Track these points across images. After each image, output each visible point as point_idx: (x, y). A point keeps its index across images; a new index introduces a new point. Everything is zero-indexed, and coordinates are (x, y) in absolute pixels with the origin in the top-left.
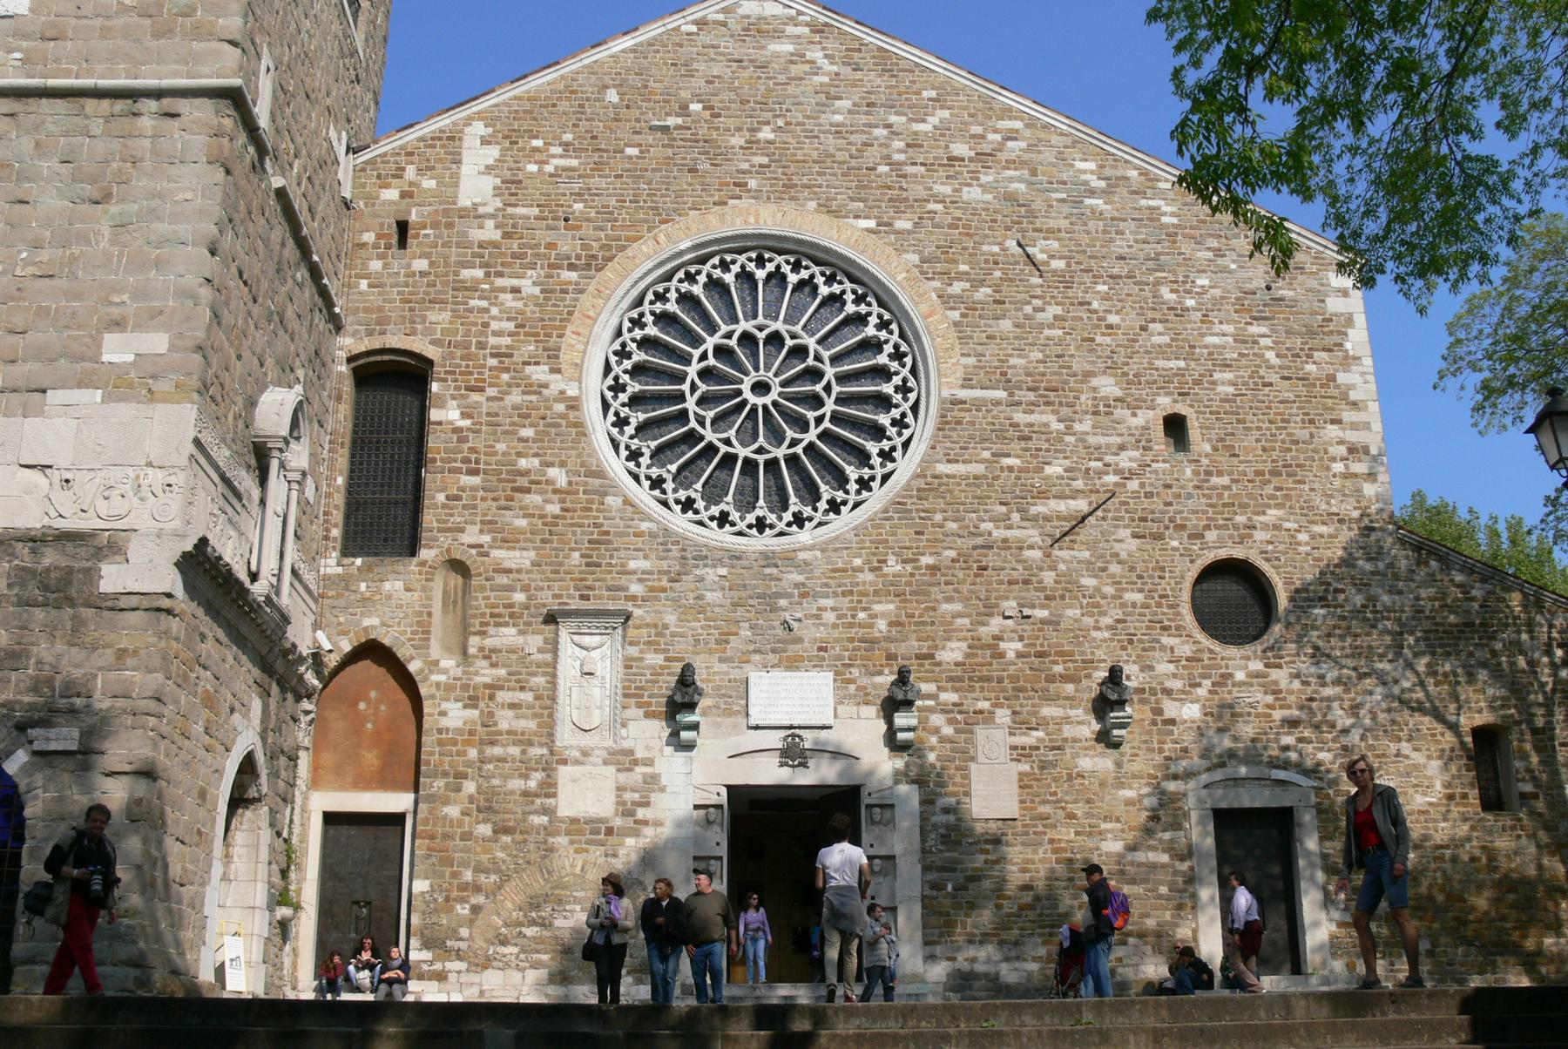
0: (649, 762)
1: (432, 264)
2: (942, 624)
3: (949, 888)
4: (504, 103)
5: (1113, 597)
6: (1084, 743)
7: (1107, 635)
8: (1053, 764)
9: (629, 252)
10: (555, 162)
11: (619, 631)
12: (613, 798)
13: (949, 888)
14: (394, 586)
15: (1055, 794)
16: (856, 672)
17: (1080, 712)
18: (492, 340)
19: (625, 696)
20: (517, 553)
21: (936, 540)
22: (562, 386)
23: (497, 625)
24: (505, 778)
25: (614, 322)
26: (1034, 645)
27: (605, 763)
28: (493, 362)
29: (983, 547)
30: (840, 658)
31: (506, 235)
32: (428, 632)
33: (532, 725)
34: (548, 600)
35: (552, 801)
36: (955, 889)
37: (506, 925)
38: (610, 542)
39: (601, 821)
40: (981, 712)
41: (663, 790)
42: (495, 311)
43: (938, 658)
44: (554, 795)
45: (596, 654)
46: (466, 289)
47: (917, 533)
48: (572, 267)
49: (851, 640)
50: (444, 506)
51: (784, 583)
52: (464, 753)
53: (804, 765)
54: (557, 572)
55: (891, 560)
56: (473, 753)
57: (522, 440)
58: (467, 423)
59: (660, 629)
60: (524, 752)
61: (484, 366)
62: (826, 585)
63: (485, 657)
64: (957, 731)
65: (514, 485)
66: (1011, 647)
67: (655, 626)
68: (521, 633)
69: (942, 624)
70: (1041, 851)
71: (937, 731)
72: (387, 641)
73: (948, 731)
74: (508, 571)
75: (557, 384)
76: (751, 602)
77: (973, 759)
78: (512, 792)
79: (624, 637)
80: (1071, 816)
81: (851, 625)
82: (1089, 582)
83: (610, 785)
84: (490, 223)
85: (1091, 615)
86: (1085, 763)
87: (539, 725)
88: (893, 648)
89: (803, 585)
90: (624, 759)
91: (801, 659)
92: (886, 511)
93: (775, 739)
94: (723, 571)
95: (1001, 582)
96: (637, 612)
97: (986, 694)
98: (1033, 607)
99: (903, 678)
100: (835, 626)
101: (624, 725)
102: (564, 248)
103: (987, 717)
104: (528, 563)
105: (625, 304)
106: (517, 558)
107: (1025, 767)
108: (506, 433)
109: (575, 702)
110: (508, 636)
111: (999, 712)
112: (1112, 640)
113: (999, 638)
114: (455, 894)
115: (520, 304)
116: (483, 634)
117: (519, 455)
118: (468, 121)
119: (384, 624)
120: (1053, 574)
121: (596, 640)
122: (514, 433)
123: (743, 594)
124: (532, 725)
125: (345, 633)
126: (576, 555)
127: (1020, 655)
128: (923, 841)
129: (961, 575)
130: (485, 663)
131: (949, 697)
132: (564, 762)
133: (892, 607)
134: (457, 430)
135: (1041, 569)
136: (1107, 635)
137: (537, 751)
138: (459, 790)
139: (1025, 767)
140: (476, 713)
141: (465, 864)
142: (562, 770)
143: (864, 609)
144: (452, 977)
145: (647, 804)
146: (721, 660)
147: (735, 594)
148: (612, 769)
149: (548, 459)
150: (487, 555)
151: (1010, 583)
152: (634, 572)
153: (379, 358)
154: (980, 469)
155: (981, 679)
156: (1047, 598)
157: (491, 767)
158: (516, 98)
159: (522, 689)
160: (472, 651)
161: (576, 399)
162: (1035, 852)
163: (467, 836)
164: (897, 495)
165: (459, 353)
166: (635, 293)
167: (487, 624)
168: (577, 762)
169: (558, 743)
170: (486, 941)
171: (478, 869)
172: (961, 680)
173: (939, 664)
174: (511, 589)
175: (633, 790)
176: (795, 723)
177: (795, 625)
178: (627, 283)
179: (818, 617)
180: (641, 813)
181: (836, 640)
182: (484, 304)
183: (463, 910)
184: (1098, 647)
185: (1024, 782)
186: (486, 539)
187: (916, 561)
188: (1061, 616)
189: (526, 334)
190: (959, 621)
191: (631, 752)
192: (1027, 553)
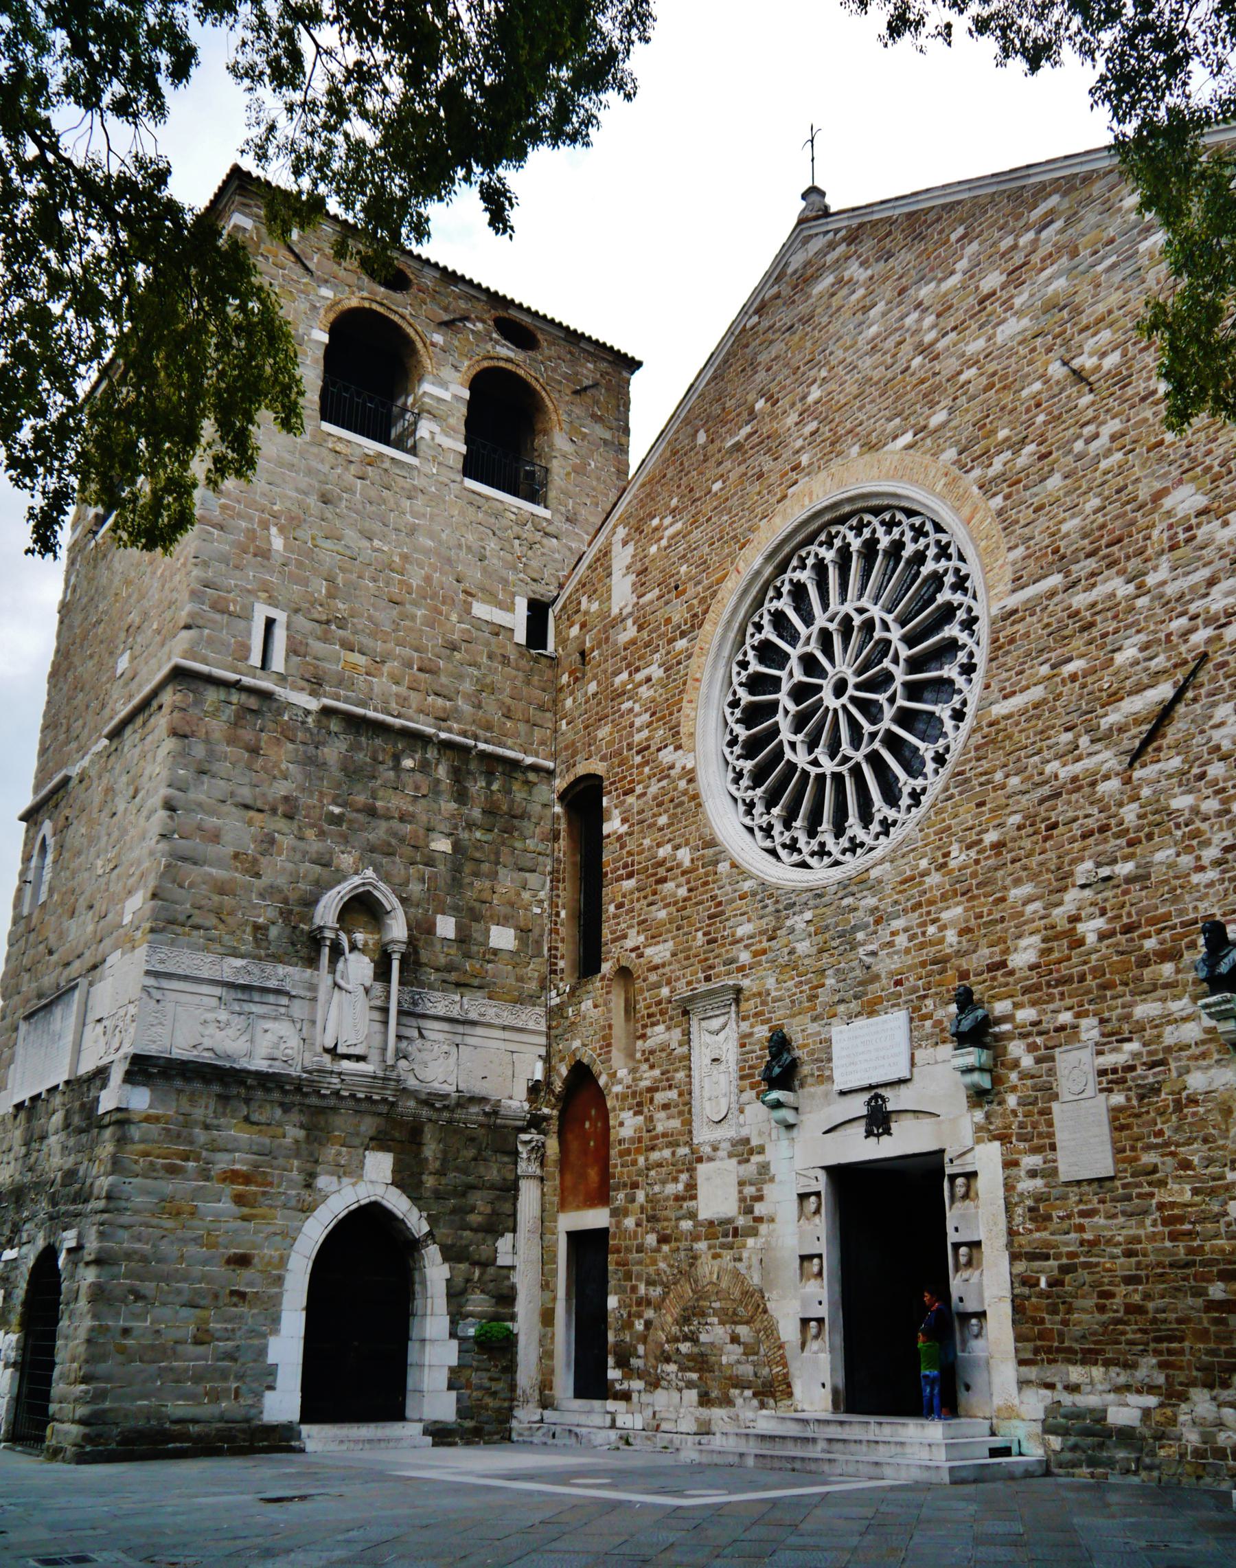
0: (761, 1150)
1: (599, 684)
2: (1013, 917)
3: (1043, 1284)
4: (635, 496)
5: (1219, 814)
6: (1195, 1051)
7: (1212, 874)
8: (1157, 1091)
9: (719, 596)
10: (668, 533)
11: (733, 1008)
12: (735, 1196)
13: (1043, 1284)
14: (587, 1005)
15: (1160, 1133)
16: (929, 1002)
17: (1186, 1000)
18: (638, 738)
19: (742, 1078)
20: (660, 947)
21: (1000, 807)
22: (683, 761)
23: (653, 1024)
24: (664, 1182)
25: (721, 672)
26: (1119, 917)
27: (730, 1155)
28: (638, 759)
29: (1049, 798)
30: (915, 990)
31: (640, 629)
32: (609, 1045)
33: (676, 1123)
34: (683, 991)
35: (693, 1203)
36: (1050, 1285)
37: (668, 1341)
38: (722, 913)
39: (729, 1221)
40: (1062, 1028)
41: (772, 1180)
42: (637, 708)
43: (1011, 965)
44: (694, 1197)
45: (722, 1035)
46: (619, 696)
47: (981, 804)
48: (683, 634)
49: (923, 964)
50: (616, 916)
51: (860, 914)
52: (634, 1163)
53: (888, 1132)
54: (687, 958)
55: (955, 850)
56: (641, 1160)
57: (661, 829)
58: (626, 826)
59: (762, 995)
60: (673, 1154)
61: (632, 767)
62: (896, 902)
63: (647, 1060)
64: (1038, 1061)
65: (658, 873)
66: (1090, 929)
67: (760, 994)
68: (668, 1028)
69: (1013, 917)
70: (1148, 1222)
71: (1016, 1064)
72: (585, 1060)
73: (1027, 1061)
74: (656, 968)
75: (683, 760)
76: (834, 944)
77: (1055, 1097)
78: (667, 1199)
79: (738, 1013)
80: (1186, 1165)
81: (922, 946)
82: (1182, 802)
83: (734, 1181)
84: (630, 622)
85: (1189, 849)
86: (1196, 1081)
87: (683, 1124)
88: (964, 964)
89: (877, 908)
90: (744, 1150)
91: (878, 1000)
92: (946, 789)
93: (858, 1106)
94: (808, 915)
95: (1073, 840)
96: (745, 983)
97: (1068, 1002)
98: (1114, 861)
99: (965, 1000)
100: (907, 951)
101: (742, 1111)
102: (676, 619)
103: (1068, 1033)
104: (668, 954)
105: (726, 653)
106: (659, 952)
107: (1118, 1099)
108: (650, 826)
109: (706, 1094)
110: (659, 1034)
111: (1085, 1023)
112: (1222, 880)
113: (1075, 919)
114: (634, 1309)
115: (651, 692)
116: (643, 1037)
117: (659, 845)
118: (613, 532)
119: (584, 1045)
120: (1135, 805)
121: (722, 1020)
122: (654, 824)
123: (827, 935)
124: (676, 1123)
125: (562, 1060)
126: (700, 934)
127: (1102, 936)
128: (1010, 1218)
129: (1027, 843)
130: (645, 1067)
131: (1026, 1015)
132: (700, 1160)
133: (959, 910)
134: (620, 838)
135: (1120, 805)
136: (1212, 874)
137: (683, 1151)
138: (633, 1201)
139: (1118, 1099)
140: (641, 1118)
141: (639, 1278)
142: (702, 1168)
143: (934, 921)
144: (635, 1396)
145: (760, 1198)
146: (814, 1019)
147: (820, 938)
148: (734, 1161)
149: (678, 841)
150: (641, 956)
151: (1084, 837)
152: (742, 940)
153: (578, 789)
154: (1037, 693)
155: (1061, 982)
156: (1131, 844)
157: (652, 1173)
158: (643, 485)
159: (670, 1087)
160: (638, 1055)
161: (693, 770)
162: (1141, 1224)
163: (640, 1249)
164: (957, 765)
165: (616, 761)
166: (732, 635)
167: (645, 1026)
168: (711, 1159)
169: (695, 1141)
170: (656, 1358)
171: (650, 1283)
172: (1037, 988)
173: (1011, 973)
174: (657, 986)
175: (751, 1184)
176: (874, 1081)
177: (868, 960)
178: (719, 630)
179: (890, 944)
180: (759, 1209)
181: (911, 968)
182: (627, 705)
183: (639, 1326)
184: (1200, 899)
185: (1119, 1121)
186: (642, 938)
187: (981, 841)
188: (1148, 865)
189: (659, 720)
190: (1030, 908)
191: (747, 1141)
192: (1102, 788)
